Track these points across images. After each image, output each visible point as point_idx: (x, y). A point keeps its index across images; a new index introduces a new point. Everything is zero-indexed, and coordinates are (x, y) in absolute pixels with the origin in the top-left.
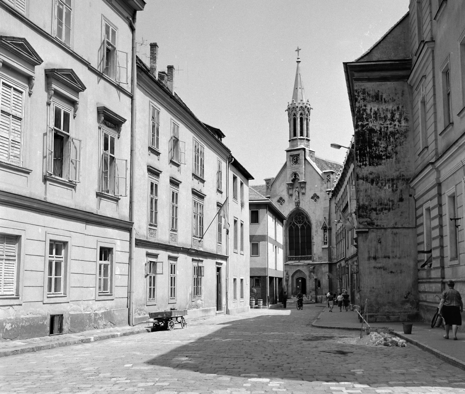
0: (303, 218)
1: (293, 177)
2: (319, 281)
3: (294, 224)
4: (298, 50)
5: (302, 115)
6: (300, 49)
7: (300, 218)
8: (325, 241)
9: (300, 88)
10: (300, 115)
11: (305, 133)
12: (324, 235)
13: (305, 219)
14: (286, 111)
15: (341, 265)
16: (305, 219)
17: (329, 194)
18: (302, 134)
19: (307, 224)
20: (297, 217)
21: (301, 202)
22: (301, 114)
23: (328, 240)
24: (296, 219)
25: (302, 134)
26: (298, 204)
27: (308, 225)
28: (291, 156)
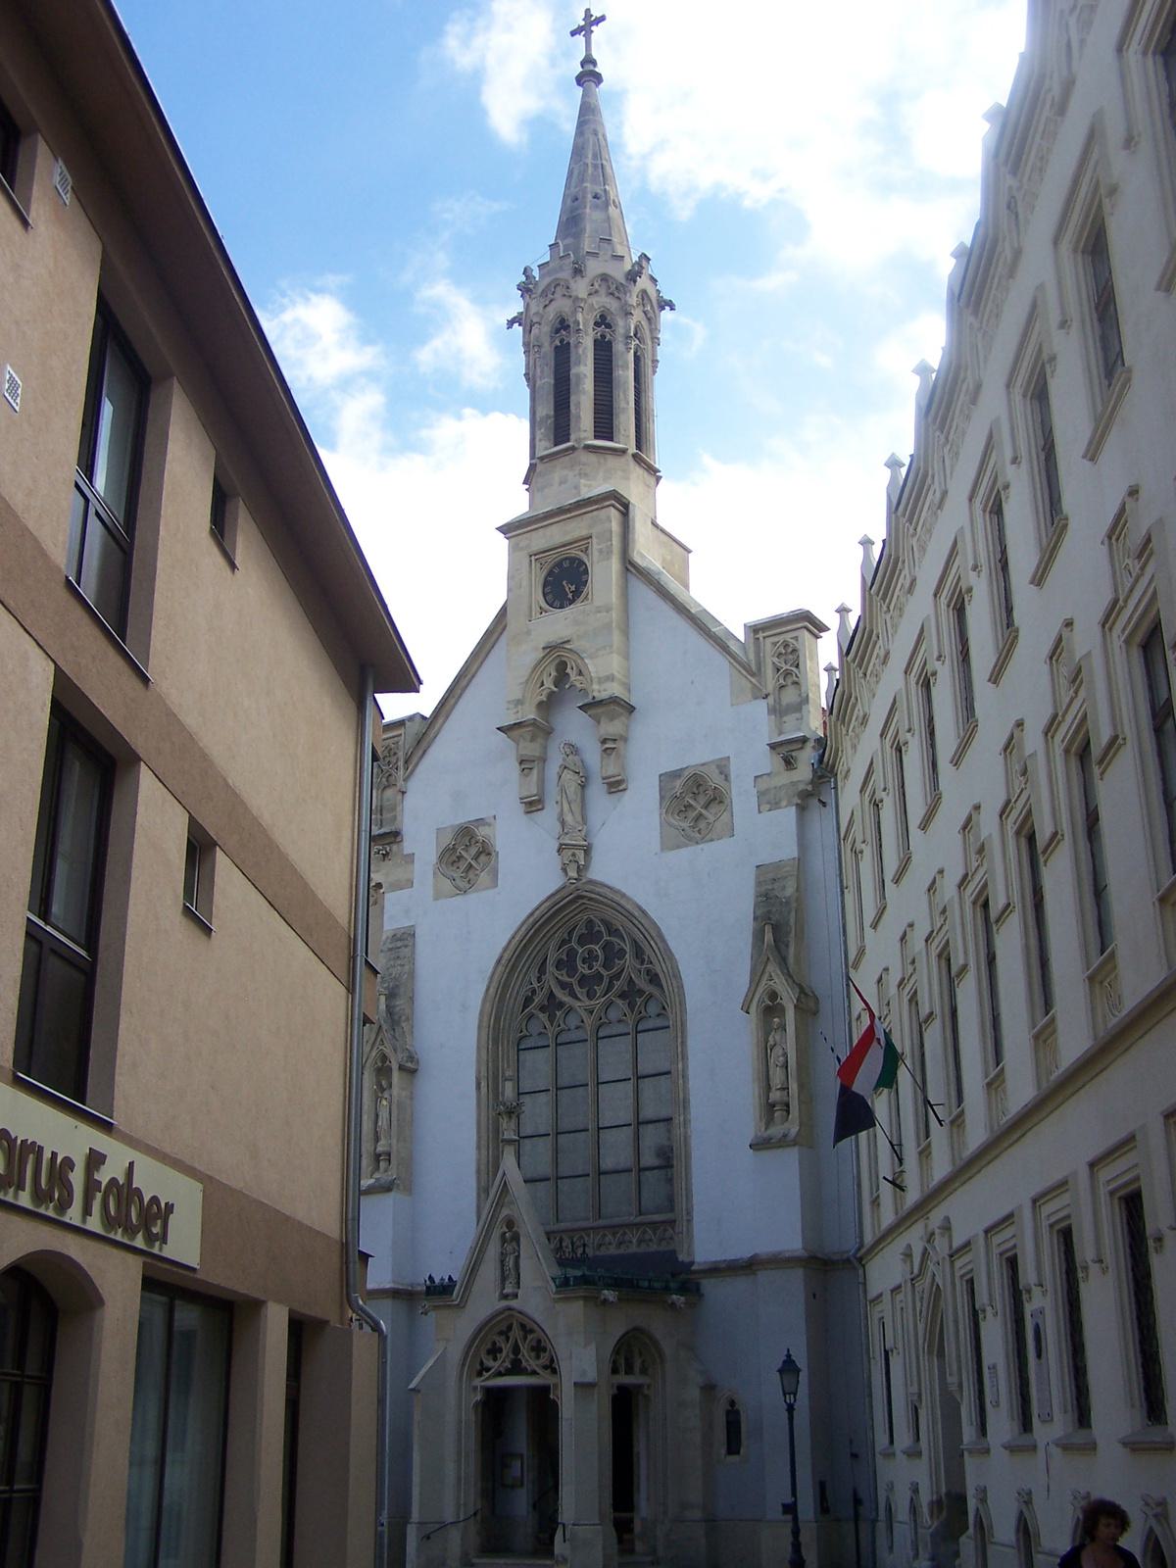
0: (612, 954)
1: (549, 684)
2: (732, 1403)
3: (552, 1005)
4: (591, 22)
5: (609, 326)
6: (596, 14)
7: (589, 959)
8: (775, 1096)
9: (596, 197)
10: (597, 324)
11: (626, 421)
12: (766, 1050)
13: (629, 957)
14: (510, 323)
15: (947, 1227)
16: (629, 957)
17: (789, 763)
18: (605, 426)
19: (641, 992)
20: (572, 954)
21: (601, 842)
22: (603, 321)
23: (794, 1086)
24: (567, 964)
25: (605, 426)
26: (576, 851)
27: (651, 996)
28: (537, 556)
